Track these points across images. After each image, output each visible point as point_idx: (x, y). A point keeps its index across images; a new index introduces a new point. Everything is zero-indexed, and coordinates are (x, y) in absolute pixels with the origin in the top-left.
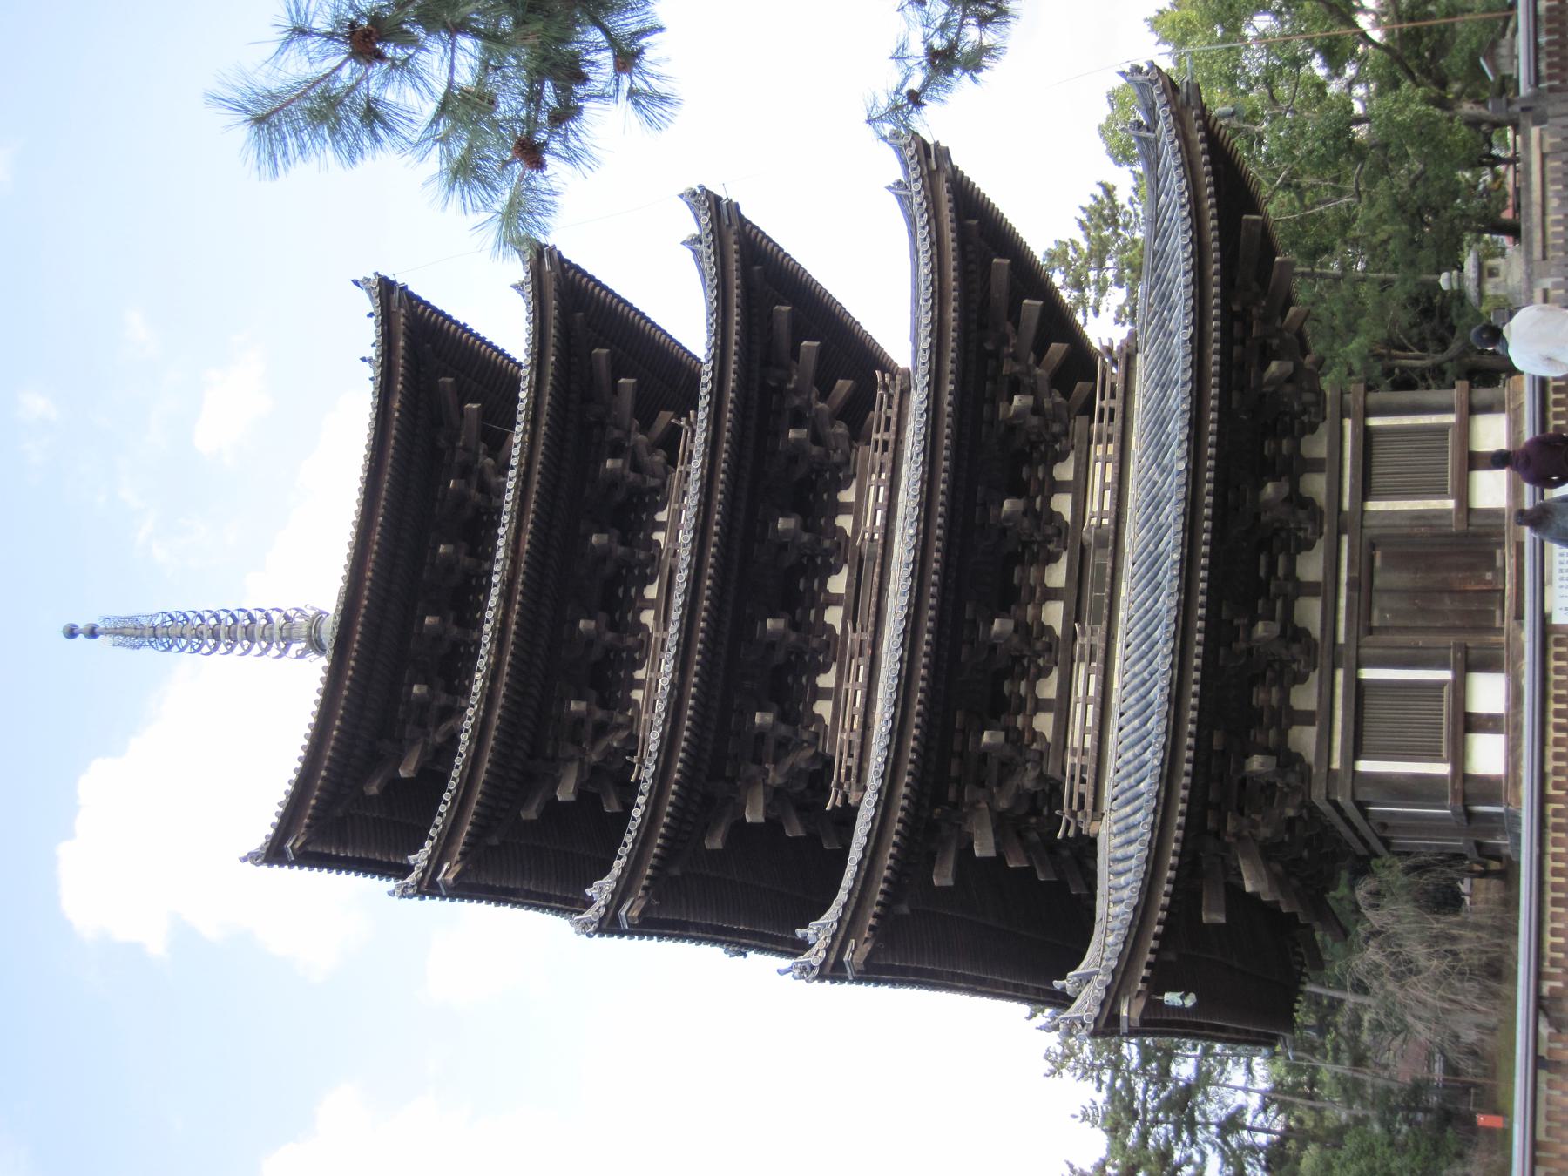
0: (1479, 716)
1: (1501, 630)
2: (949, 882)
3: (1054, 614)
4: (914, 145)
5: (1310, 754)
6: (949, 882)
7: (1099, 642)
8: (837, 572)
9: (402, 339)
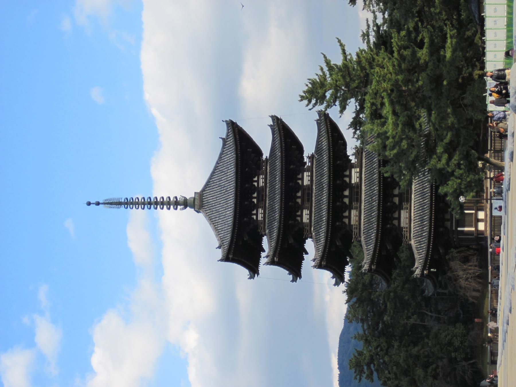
0: (480, 219)
1: (483, 203)
5: (449, 227)
7: (408, 206)
8: (346, 190)
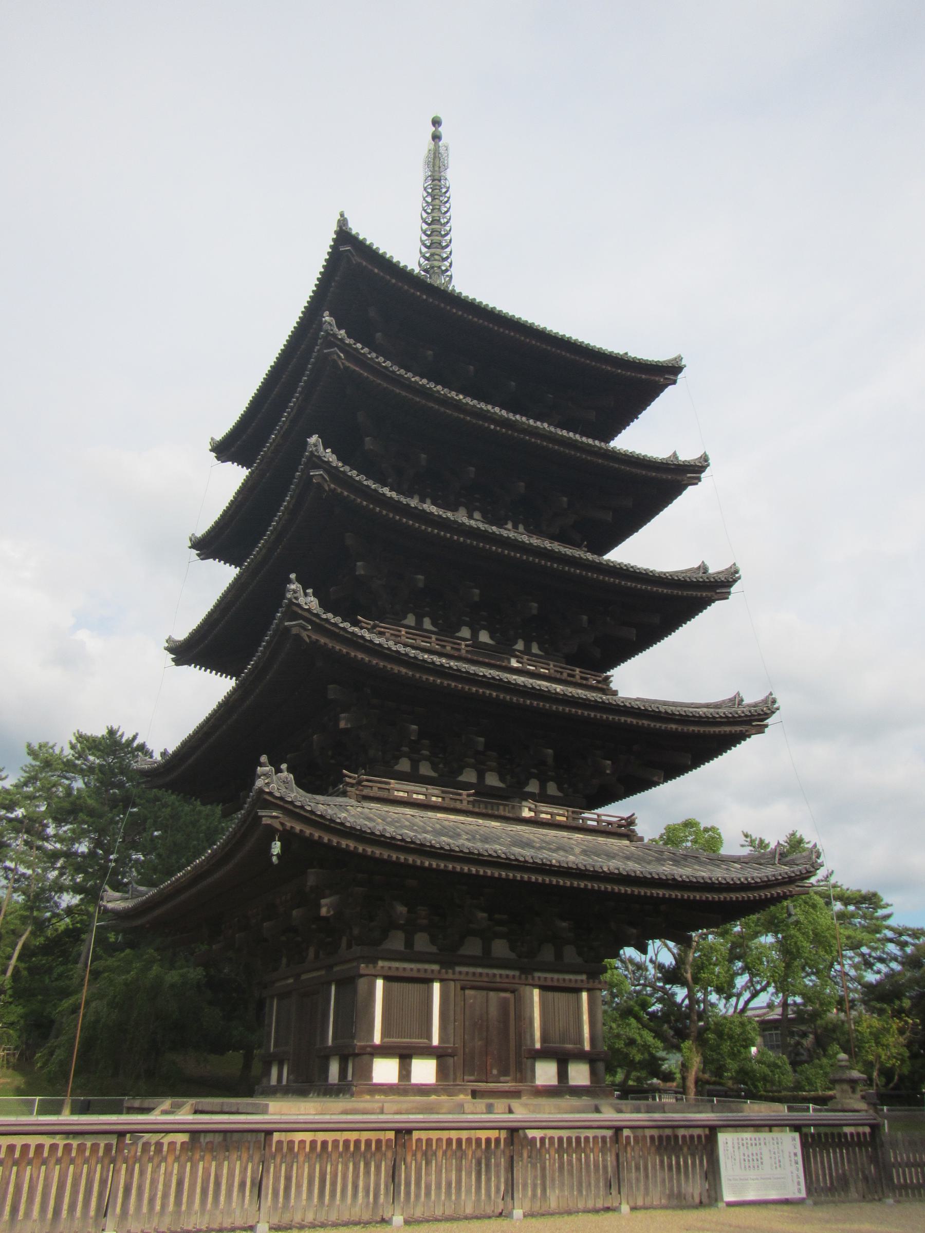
0: (410, 1065)
2: (331, 696)
3: (470, 776)
4: (768, 712)
6: (331, 696)
7: (464, 806)
8: (492, 638)
9: (648, 377)
